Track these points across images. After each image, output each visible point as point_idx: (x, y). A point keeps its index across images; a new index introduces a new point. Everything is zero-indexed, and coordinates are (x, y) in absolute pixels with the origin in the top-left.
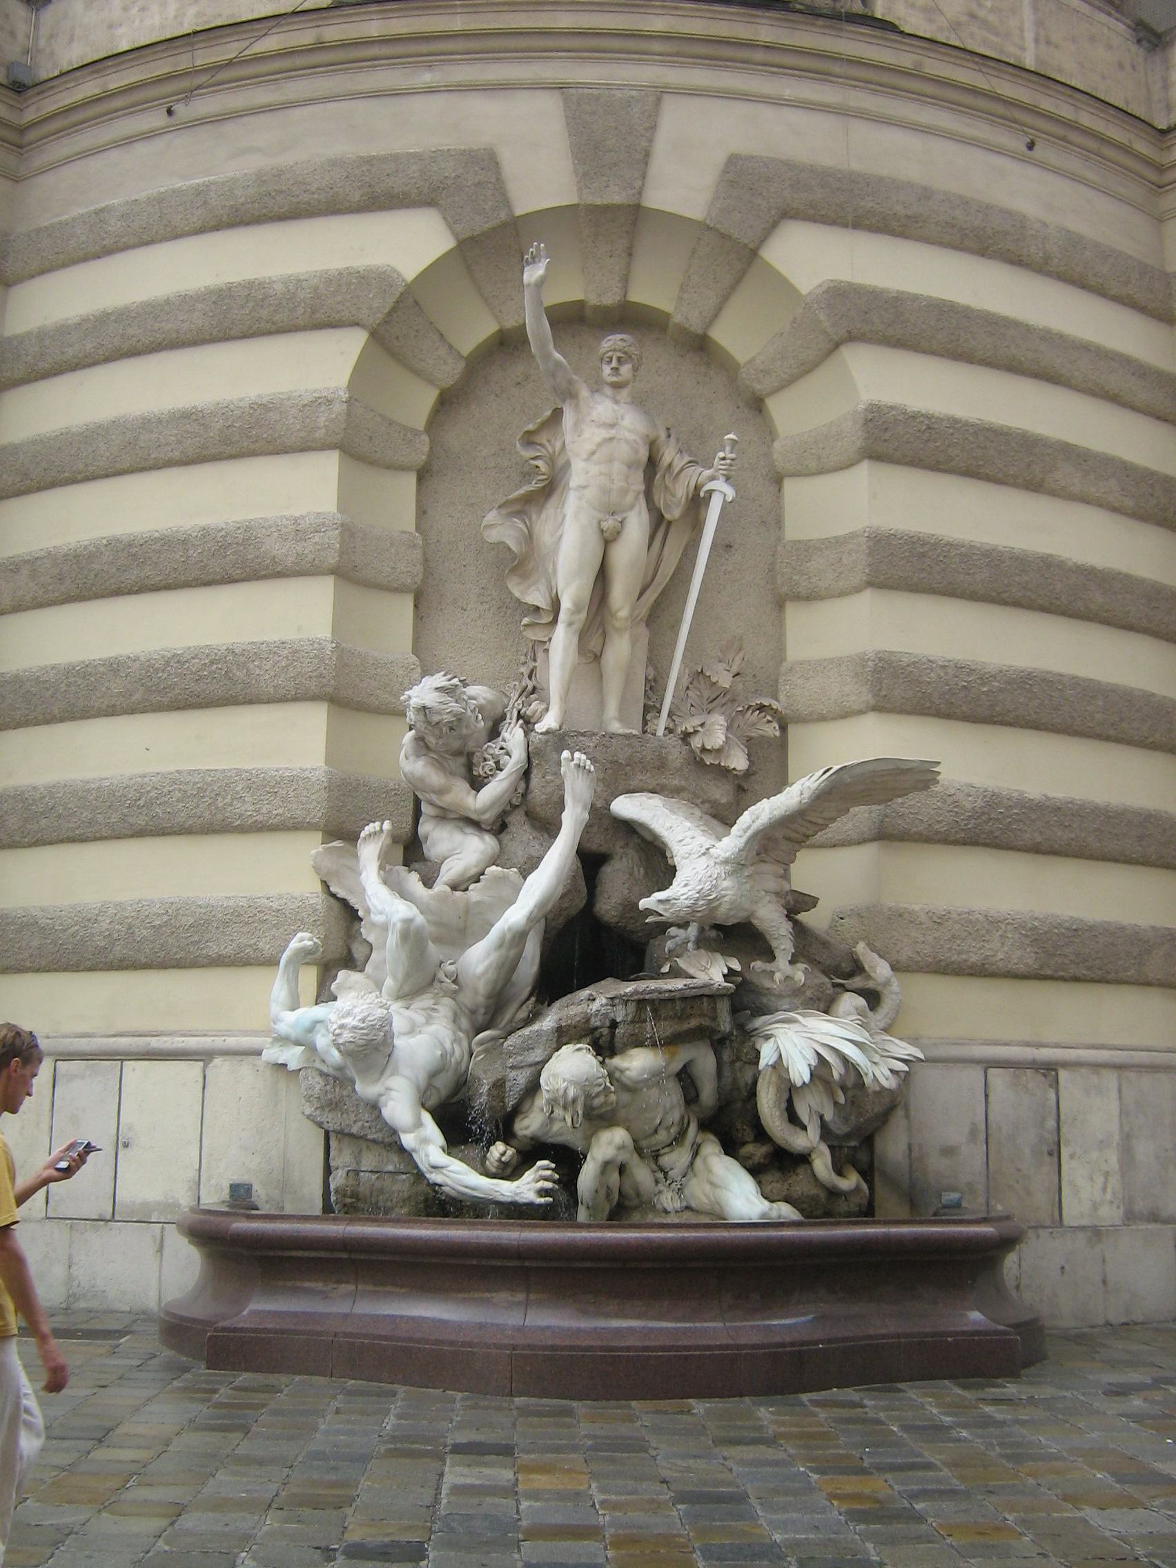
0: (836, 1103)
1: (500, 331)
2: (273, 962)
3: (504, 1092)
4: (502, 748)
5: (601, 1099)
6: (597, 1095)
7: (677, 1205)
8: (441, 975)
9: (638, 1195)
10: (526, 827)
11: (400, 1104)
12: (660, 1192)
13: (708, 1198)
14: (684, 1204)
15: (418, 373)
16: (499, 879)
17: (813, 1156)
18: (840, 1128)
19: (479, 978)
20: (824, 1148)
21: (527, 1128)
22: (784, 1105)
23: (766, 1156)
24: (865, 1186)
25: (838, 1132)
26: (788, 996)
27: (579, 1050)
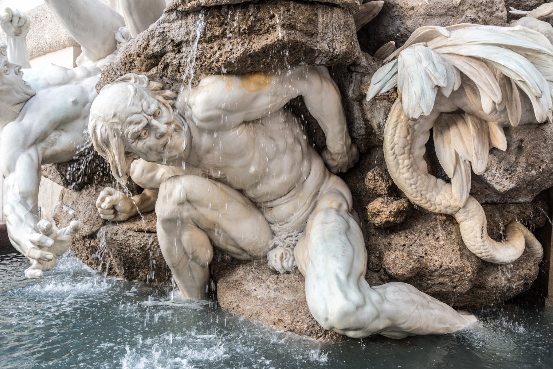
0: (493, 150)
5: (150, 141)
6: (138, 137)
7: (288, 264)
8: (119, 37)
9: (244, 250)
12: (275, 246)
18: (503, 184)
20: (475, 207)
22: (420, 151)
23: (399, 213)
24: (538, 247)
25: (498, 188)
26: (441, 16)
27: (124, 80)
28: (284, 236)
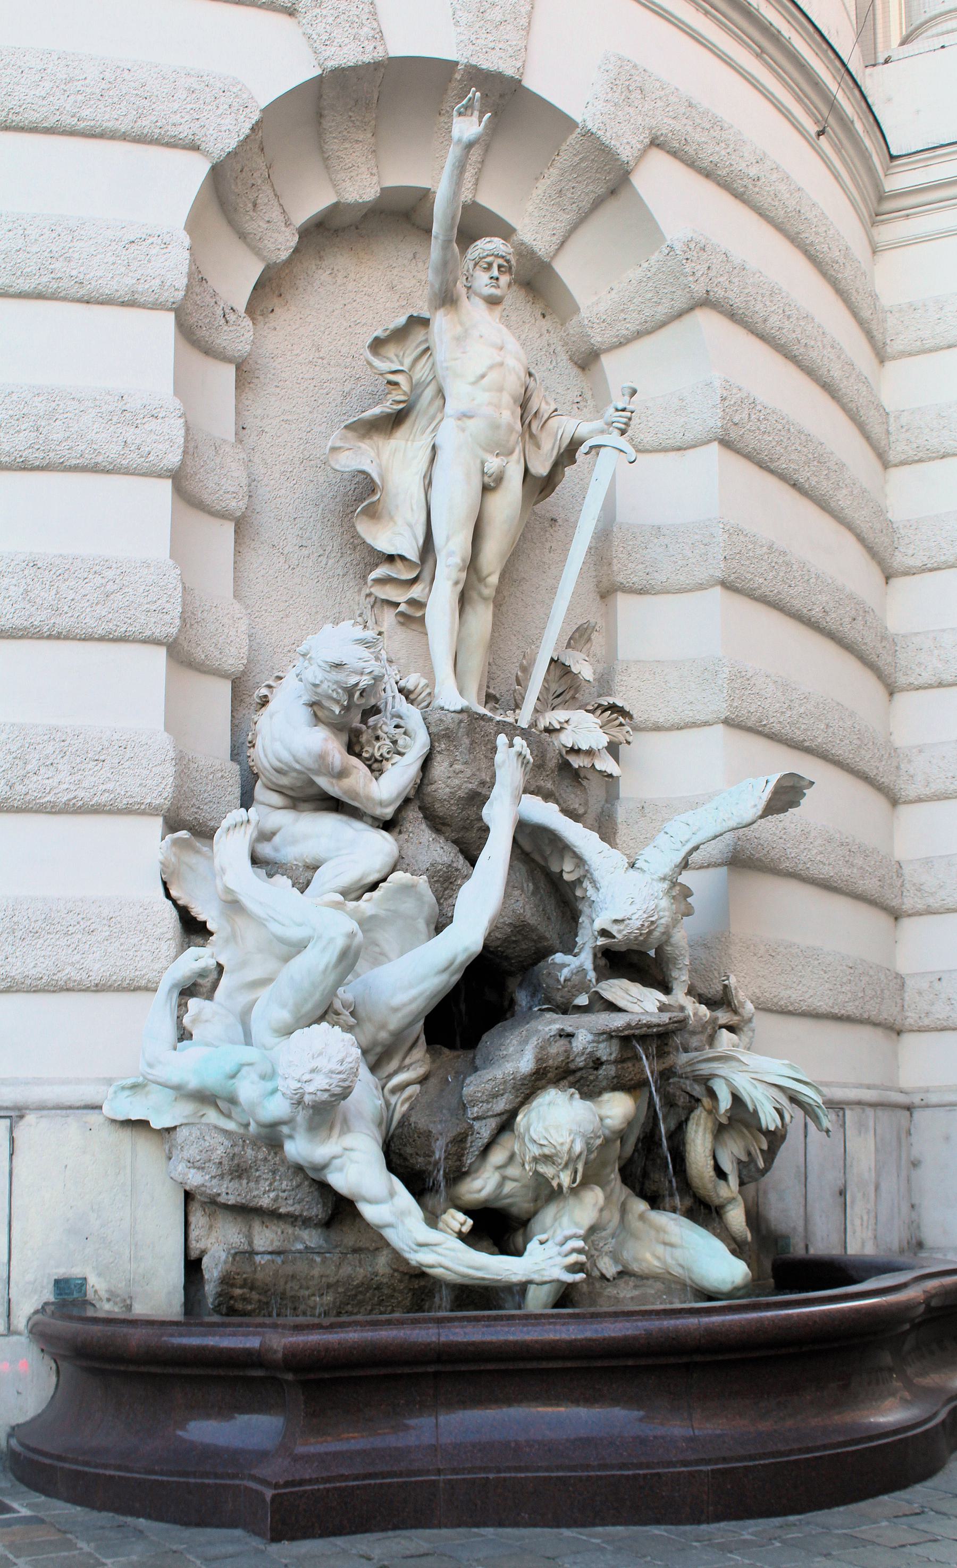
1: (336, 206)
2: (150, 989)
3: (464, 1149)
4: (397, 726)
10: (424, 826)
11: (358, 1166)
13: (665, 1263)
14: (620, 1268)
15: (243, 236)
16: (407, 889)
17: (729, 1207)
19: (396, 1010)
21: (480, 1191)
28: (601, 1245)
